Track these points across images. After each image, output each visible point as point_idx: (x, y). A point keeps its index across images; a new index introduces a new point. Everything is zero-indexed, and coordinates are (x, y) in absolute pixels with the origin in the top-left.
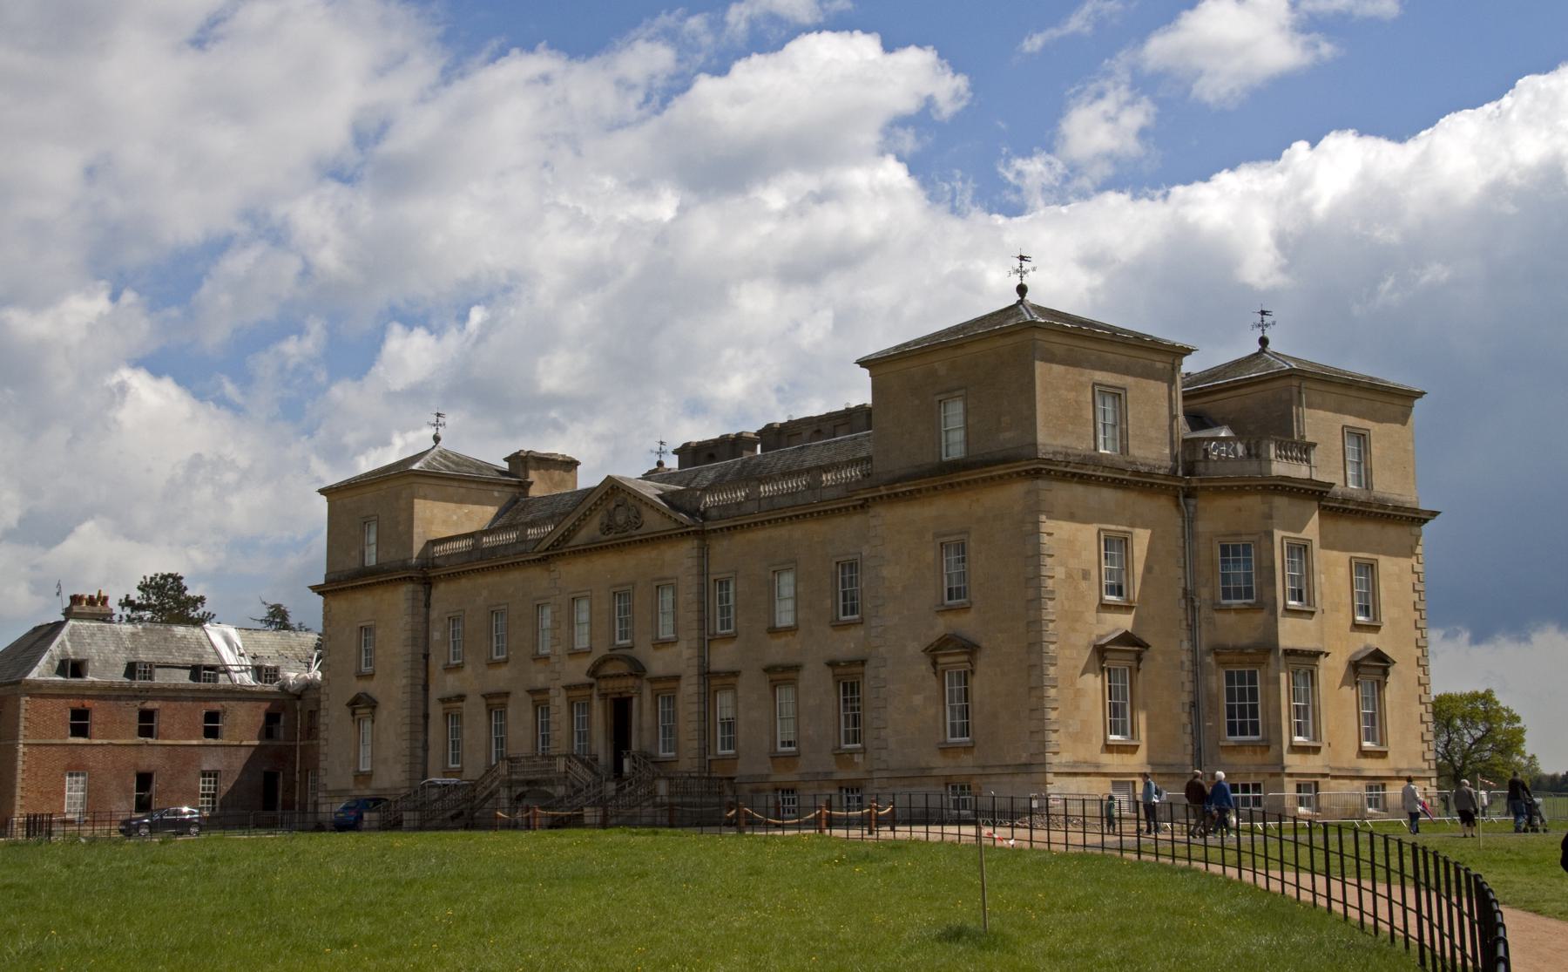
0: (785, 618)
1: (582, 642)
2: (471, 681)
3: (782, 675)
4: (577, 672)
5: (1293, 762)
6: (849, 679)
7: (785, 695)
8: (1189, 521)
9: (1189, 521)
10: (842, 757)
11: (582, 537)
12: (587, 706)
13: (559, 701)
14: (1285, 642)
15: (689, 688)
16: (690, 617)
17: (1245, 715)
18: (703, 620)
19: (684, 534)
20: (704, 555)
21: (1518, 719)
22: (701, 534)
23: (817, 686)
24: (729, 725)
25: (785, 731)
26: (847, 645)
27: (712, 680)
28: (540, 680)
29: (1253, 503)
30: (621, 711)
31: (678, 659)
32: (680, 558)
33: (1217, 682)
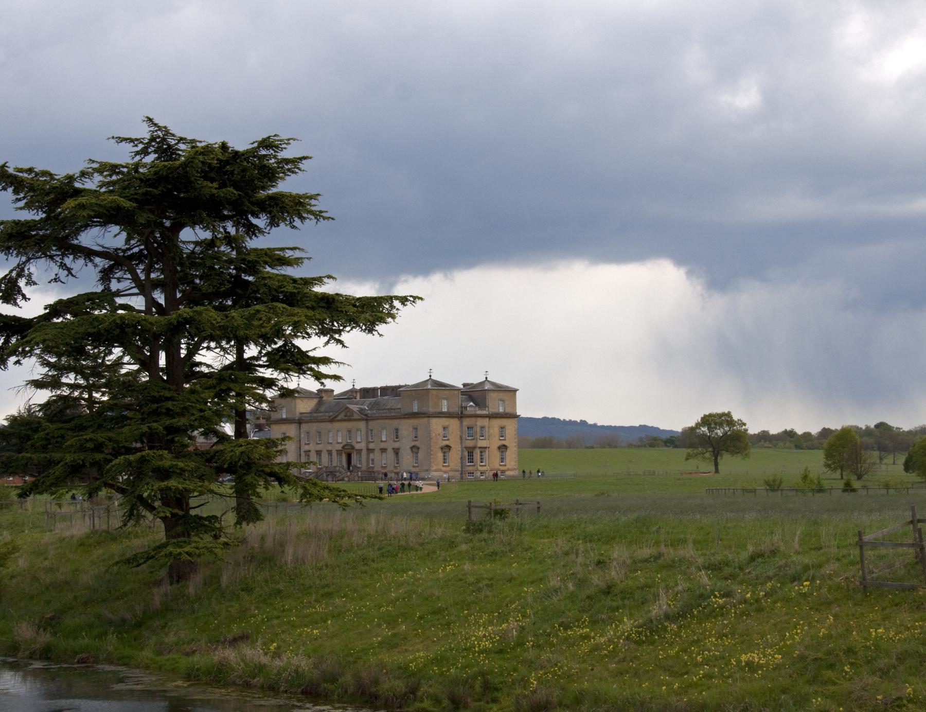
0: (384, 439)
1: (340, 441)
2: (312, 447)
3: (383, 450)
4: (339, 447)
5: (480, 468)
6: (396, 452)
7: (384, 455)
8: (461, 423)
9: (461, 423)
10: (396, 467)
11: (339, 418)
12: (341, 455)
13: (334, 454)
14: (479, 445)
15: (364, 453)
16: (364, 437)
17: (471, 460)
18: (367, 438)
19: (363, 420)
20: (367, 424)
21: (745, 424)
22: (367, 420)
23: (390, 453)
24: (373, 460)
25: (384, 462)
26: (396, 445)
27: (370, 451)
28: (330, 448)
29: (473, 420)
30: (349, 457)
31: (362, 446)
32: (362, 425)
33: (466, 453)
